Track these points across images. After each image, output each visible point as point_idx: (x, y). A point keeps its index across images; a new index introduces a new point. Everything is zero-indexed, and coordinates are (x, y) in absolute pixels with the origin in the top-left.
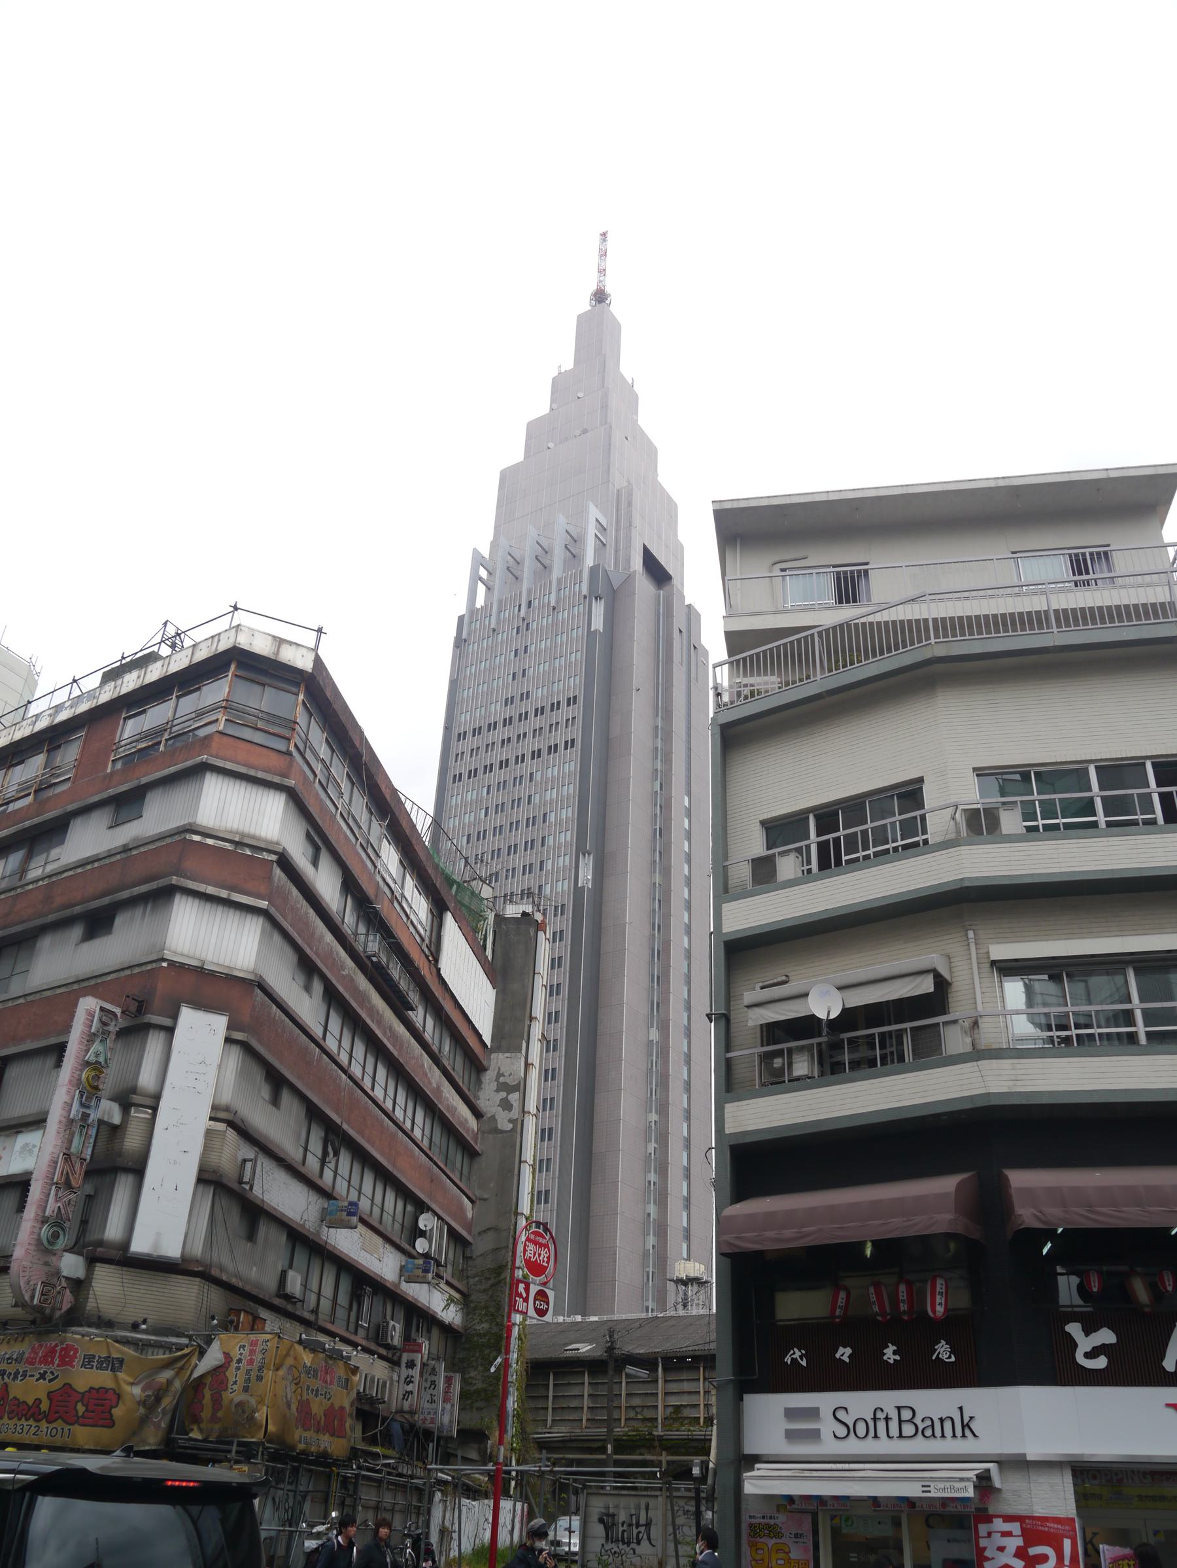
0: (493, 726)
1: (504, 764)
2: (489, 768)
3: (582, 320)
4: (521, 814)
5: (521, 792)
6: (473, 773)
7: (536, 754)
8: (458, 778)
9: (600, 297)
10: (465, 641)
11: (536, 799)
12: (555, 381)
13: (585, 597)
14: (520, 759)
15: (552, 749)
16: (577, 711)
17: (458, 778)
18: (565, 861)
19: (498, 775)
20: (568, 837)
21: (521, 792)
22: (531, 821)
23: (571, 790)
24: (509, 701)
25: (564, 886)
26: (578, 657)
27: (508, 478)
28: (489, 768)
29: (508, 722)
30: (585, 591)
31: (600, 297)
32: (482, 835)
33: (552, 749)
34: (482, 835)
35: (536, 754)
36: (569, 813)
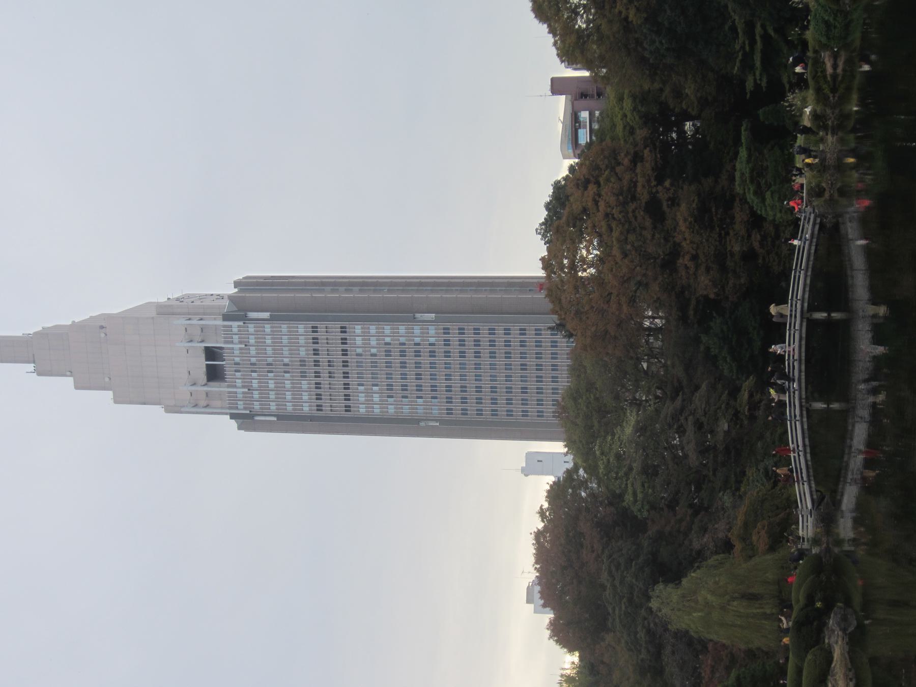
0: (318, 385)
1: (346, 375)
2: (346, 386)
6: (347, 397)
7: (345, 352)
8: (348, 409)
10: (250, 411)
11: (374, 351)
12: (39, 374)
13: (244, 323)
14: (345, 364)
15: (344, 341)
16: (321, 326)
17: (348, 409)
18: (417, 331)
19: (353, 381)
20: (402, 330)
22: (388, 353)
23: (373, 329)
26: (284, 328)
28: (346, 386)
29: (317, 375)
30: (241, 323)
32: (390, 387)
33: (344, 341)
34: (390, 387)
35: (345, 352)
36: (387, 330)
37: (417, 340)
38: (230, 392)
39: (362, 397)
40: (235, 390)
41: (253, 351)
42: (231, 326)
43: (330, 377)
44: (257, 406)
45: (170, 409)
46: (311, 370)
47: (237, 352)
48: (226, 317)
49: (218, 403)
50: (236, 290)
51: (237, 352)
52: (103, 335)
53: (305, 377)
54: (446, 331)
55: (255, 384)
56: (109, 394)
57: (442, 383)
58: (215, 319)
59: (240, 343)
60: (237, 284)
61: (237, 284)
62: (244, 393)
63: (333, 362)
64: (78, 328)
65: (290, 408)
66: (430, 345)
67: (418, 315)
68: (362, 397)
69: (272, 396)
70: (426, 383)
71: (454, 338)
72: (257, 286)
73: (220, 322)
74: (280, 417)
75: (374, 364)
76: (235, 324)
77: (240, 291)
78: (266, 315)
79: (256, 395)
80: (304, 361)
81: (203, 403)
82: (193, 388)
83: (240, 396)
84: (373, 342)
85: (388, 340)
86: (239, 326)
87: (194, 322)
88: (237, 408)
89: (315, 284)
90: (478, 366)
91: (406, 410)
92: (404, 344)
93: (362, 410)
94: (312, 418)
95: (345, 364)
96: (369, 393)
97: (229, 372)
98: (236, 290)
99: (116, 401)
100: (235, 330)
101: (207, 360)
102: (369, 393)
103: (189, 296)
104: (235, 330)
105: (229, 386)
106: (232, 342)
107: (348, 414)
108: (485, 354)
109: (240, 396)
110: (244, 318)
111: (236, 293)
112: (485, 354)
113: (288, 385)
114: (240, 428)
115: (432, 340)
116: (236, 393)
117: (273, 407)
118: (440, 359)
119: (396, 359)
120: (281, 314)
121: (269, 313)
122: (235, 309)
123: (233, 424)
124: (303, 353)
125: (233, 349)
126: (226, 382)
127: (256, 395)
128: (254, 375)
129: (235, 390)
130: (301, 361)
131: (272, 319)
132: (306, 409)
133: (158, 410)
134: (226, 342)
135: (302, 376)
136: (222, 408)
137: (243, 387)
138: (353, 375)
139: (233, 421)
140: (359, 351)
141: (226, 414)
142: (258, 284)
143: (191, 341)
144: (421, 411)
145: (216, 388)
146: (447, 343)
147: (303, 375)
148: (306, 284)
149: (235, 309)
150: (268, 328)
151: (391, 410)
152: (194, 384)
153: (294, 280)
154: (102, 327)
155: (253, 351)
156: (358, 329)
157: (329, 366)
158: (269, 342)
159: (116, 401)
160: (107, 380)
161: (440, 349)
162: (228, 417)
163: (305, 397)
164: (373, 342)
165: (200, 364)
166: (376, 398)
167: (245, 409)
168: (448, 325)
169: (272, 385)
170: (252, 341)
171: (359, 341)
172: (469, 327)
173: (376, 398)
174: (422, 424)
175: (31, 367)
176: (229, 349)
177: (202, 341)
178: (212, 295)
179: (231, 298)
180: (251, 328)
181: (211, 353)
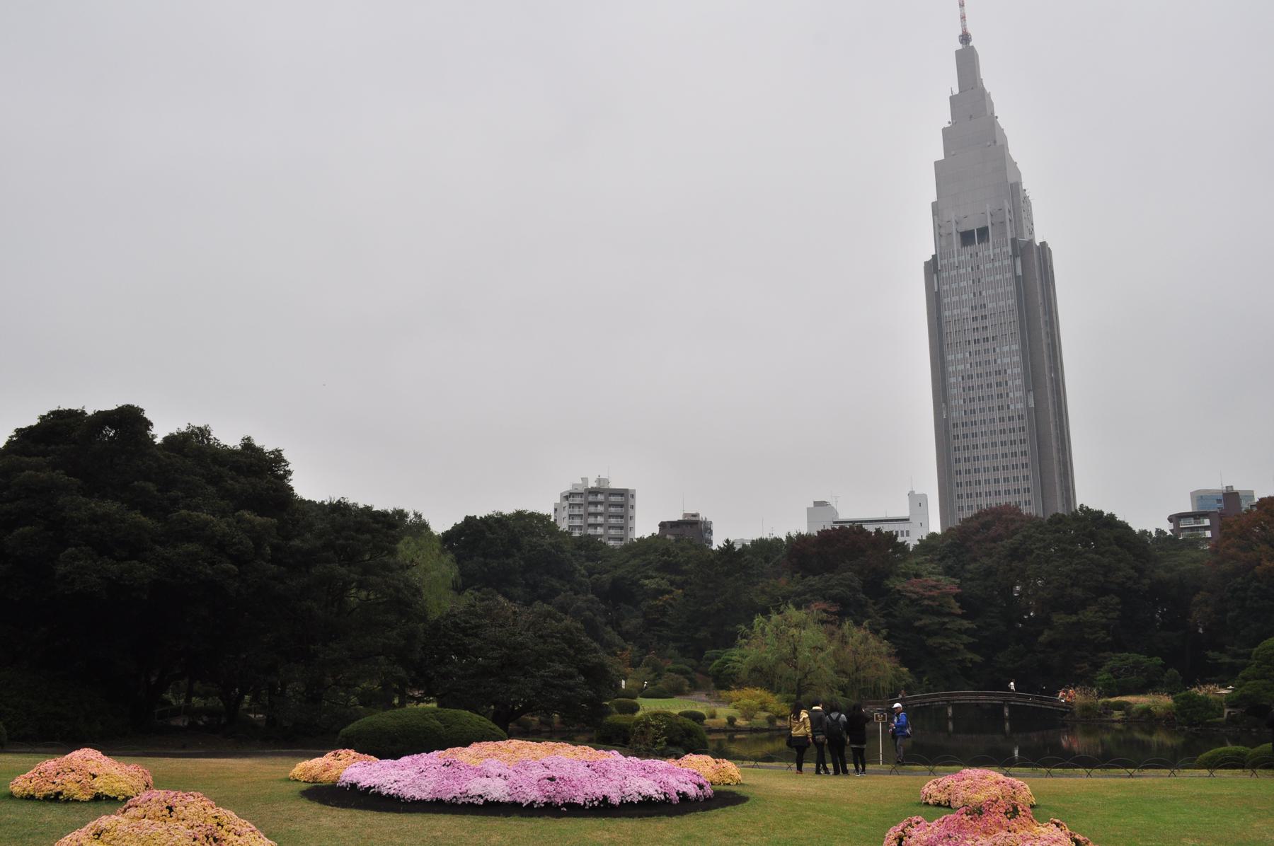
3: (959, 54)
4: (992, 368)
5: (991, 357)
9: (965, 38)
11: (999, 361)
12: (951, 98)
14: (986, 340)
18: (1019, 394)
19: (974, 347)
20: (1018, 382)
21: (991, 357)
23: (1016, 359)
24: (974, 308)
25: (1020, 406)
26: (1011, 288)
27: (938, 164)
30: (1010, 253)
31: (965, 38)
36: (1017, 370)
37: (1011, 395)
38: (953, 251)
39: (960, 356)
40: (956, 256)
41: (989, 266)
42: (1007, 245)
43: (974, 329)
44: (945, 275)
45: (935, 205)
46: (978, 313)
47: (986, 253)
48: (1014, 241)
49: (944, 243)
50: (1038, 244)
51: (986, 253)
52: (989, 144)
53: (972, 309)
54: (1021, 417)
55: (962, 271)
56: (941, 156)
57: (978, 417)
58: (1012, 231)
59: (994, 255)
60: (1043, 244)
61: (1043, 244)
62: (954, 263)
63: (987, 330)
64: (993, 119)
65: (946, 300)
66: (1008, 405)
67: (1032, 393)
68: (960, 356)
69: (954, 286)
70: (977, 405)
71: (1016, 424)
72: (1044, 261)
73: (1009, 237)
74: (938, 294)
75: (987, 362)
76: (1010, 249)
77: (1038, 247)
78: (1019, 272)
79: (953, 273)
80: (985, 307)
81: (943, 231)
82: (954, 224)
83: (951, 260)
84: (1006, 360)
85: (1009, 371)
86: (1008, 252)
87: (1008, 216)
88: (941, 259)
89: (1050, 307)
90: (994, 444)
91: (954, 391)
92: (1007, 385)
93: (950, 358)
94: (939, 318)
95: (986, 340)
96: (964, 361)
97: (969, 249)
98: (1038, 244)
99: (936, 163)
100: (1004, 250)
101: (977, 229)
102: (964, 361)
103: (1029, 205)
104: (1004, 250)
105: (958, 250)
106: (994, 248)
107: (945, 346)
108: (1005, 450)
109: (951, 260)
110: (1015, 256)
111: (1036, 245)
112: (1005, 450)
113: (964, 297)
114: (926, 263)
115: (1012, 407)
116: (954, 257)
117: (945, 287)
118: (997, 414)
119: (994, 379)
120: (1022, 287)
121: (1021, 274)
122: (1022, 247)
123: (929, 258)
124: (991, 305)
125: (989, 249)
126: (962, 247)
127: (953, 273)
128: (970, 269)
129: (956, 256)
130: (985, 305)
131: (1017, 278)
132: (946, 313)
133: (934, 198)
134: (993, 242)
135: (972, 307)
136: (940, 247)
137: (959, 262)
138: (977, 347)
139: (931, 257)
140: (998, 350)
141: (936, 251)
142: (1045, 261)
143: (992, 215)
144: (954, 403)
145: (956, 240)
146: (1011, 418)
147: (974, 308)
148: (1049, 299)
149: (1022, 247)
150: (1008, 275)
151: (953, 380)
152: (957, 223)
153: (1052, 290)
154: (995, 142)
155: (987, 266)
156: (1015, 347)
157: (983, 328)
158: (998, 277)
159: (936, 163)
160: (953, 153)
161: (1005, 414)
162: (934, 253)
163: (956, 312)
164: (1006, 360)
165: (973, 225)
166: (961, 367)
167: (942, 266)
168: (1026, 417)
169: (963, 284)
170: (997, 264)
171: (1006, 348)
172: (1025, 435)
173: (961, 367)
174: (943, 405)
175: (956, 91)
176: (989, 246)
177: (992, 224)
178: (1032, 224)
179: (1031, 242)
180: (1007, 262)
181: (983, 233)
